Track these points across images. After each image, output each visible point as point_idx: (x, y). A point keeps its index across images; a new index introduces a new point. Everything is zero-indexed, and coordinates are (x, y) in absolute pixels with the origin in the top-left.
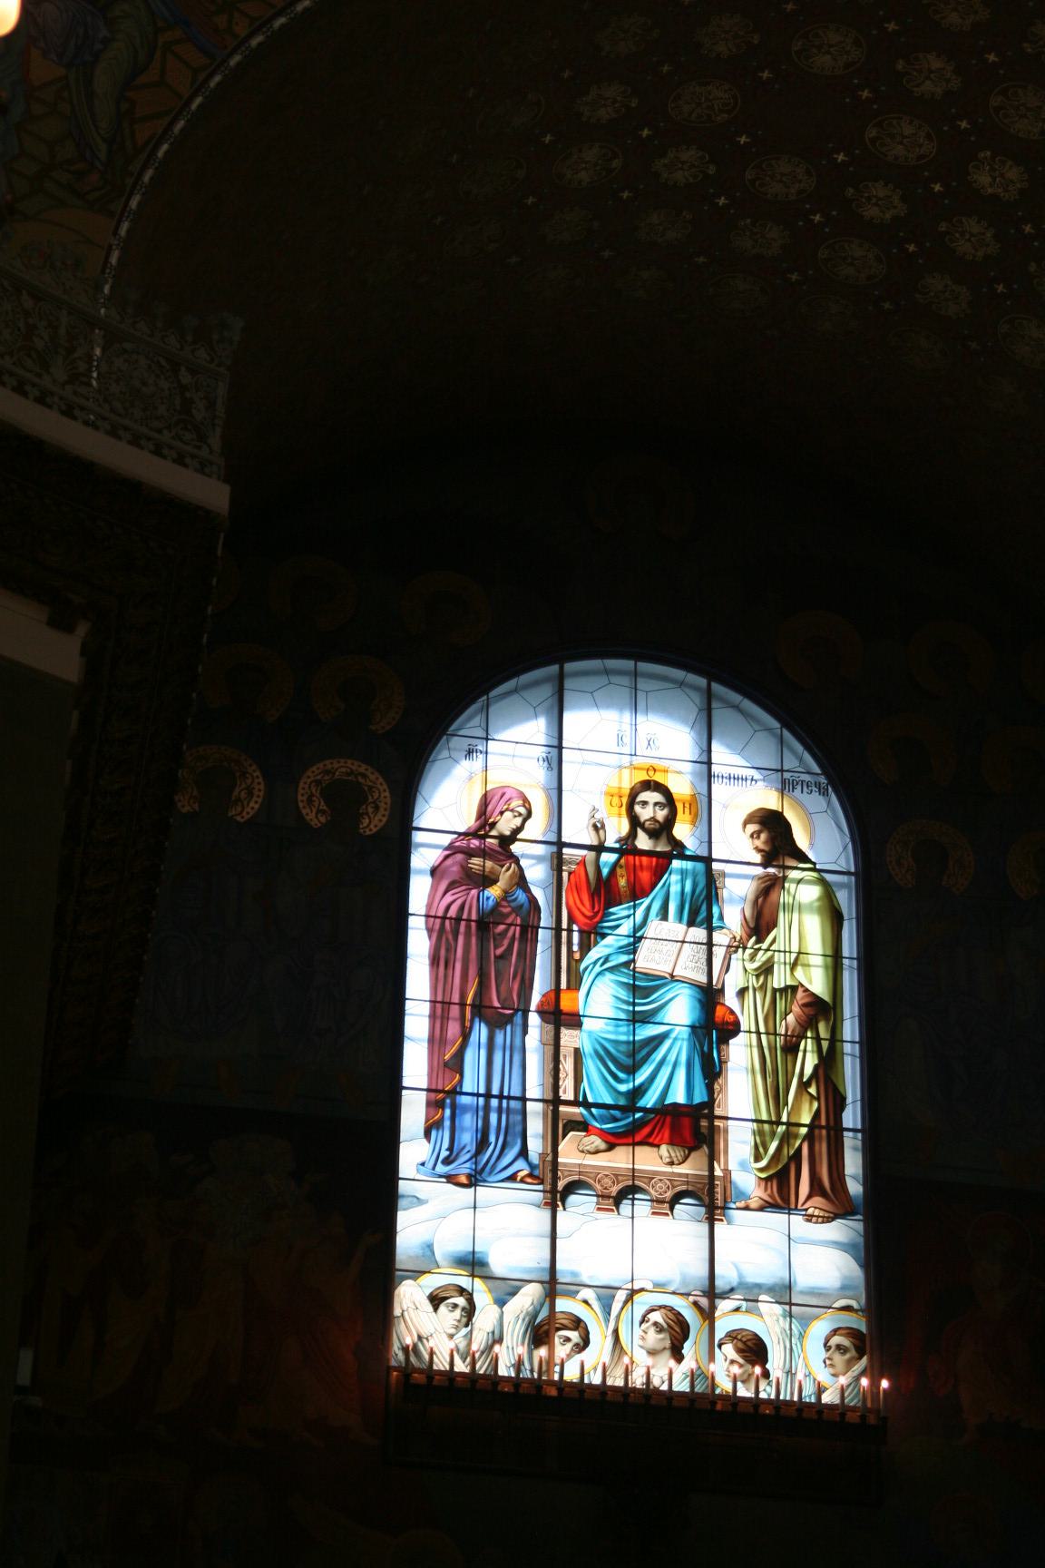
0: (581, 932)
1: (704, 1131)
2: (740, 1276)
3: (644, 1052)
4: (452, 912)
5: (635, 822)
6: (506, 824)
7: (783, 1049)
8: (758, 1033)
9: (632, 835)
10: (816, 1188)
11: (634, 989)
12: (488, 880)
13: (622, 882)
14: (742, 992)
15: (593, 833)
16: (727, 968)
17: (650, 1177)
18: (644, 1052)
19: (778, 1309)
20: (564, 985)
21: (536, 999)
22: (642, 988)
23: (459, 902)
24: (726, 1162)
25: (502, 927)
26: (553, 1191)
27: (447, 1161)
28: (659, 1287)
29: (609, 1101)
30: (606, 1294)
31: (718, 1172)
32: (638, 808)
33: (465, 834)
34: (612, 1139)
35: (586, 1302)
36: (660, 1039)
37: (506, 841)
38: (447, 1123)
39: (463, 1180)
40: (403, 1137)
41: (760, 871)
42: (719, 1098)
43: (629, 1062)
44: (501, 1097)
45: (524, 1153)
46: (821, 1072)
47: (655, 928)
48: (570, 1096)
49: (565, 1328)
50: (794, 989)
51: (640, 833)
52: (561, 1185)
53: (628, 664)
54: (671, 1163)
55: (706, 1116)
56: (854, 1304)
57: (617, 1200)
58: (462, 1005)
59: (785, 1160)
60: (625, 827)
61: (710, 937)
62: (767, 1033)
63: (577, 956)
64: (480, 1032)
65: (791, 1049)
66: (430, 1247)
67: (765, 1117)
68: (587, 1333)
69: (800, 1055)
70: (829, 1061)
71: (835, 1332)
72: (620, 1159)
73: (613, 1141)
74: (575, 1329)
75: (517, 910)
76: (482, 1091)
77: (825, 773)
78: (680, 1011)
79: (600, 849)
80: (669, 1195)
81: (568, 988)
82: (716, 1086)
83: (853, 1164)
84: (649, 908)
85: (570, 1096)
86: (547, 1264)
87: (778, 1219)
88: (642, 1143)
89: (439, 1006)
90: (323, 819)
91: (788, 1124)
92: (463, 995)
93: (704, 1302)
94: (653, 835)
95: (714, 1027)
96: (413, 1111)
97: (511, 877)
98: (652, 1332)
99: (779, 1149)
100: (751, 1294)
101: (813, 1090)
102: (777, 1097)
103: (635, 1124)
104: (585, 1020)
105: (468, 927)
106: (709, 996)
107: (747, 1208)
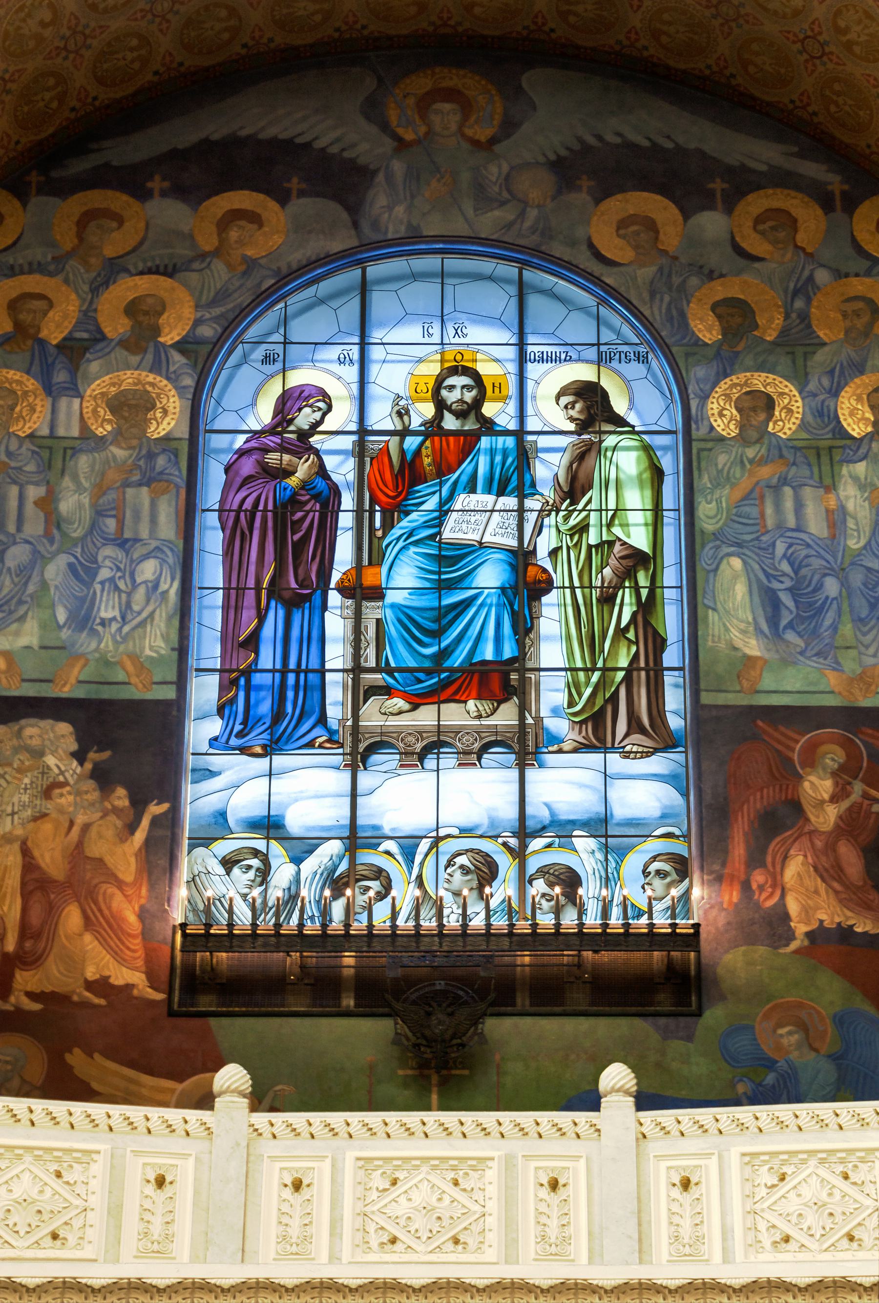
0: (383, 511)
2: (552, 813)
4: (248, 505)
5: (441, 406)
6: (304, 418)
7: (598, 600)
8: (572, 588)
10: (634, 725)
11: (440, 559)
13: (427, 461)
14: (554, 553)
15: (397, 420)
16: (539, 529)
17: (456, 731)
19: (592, 843)
21: (336, 577)
23: (255, 495)
24: (538, 710)
25: (299, 515)
26: (353, 753)
27: (241, 735)
28: (466, 832)
29: (412, 663)
31: (530, 721)
32: (444, 393)
34: (418, 701)
35: (388, 853)
36: (466, 604)
37: (304, 435)
39: (258, 750)
41: (573, 438)
43: (434, 626)
44: (297, 672)
45: (322, 720)
46: (640, 619)
47: (462, 501)
48: (372, 663)
50: (611, 544)
51: (447, 416)
54: (480, 717)
56: (677, 832)
57: (421, 759)
58: (258, 588)
61: (521, 504)
62: (582, 587)
63: (379, 534)
65: (608, 599)
66: (222, 814)
67: (579, 664)
69: (616, 609)
71: (654, 859)
72: (426, 717)
73: (416, 702)
75: (316, 497)
76: (278, 666)
78: (490, 576)
79: (404, 433)
80: (477, 746)
81: (370, 563)
82: (527, 641)
85: (372, 663)
86: (348, 822)
87: (595, 759)
89: (233, 593)
90: (109, 428)
91: (604, 670)
93: (513, 842)
94: (460, 415)
96: (204, 691)
98: (458, 876)
99: (593, 694)
101: (631, 635)
102: (592, 644)
104: (389, 593)
106: (521, 558)
107: (560, 751)
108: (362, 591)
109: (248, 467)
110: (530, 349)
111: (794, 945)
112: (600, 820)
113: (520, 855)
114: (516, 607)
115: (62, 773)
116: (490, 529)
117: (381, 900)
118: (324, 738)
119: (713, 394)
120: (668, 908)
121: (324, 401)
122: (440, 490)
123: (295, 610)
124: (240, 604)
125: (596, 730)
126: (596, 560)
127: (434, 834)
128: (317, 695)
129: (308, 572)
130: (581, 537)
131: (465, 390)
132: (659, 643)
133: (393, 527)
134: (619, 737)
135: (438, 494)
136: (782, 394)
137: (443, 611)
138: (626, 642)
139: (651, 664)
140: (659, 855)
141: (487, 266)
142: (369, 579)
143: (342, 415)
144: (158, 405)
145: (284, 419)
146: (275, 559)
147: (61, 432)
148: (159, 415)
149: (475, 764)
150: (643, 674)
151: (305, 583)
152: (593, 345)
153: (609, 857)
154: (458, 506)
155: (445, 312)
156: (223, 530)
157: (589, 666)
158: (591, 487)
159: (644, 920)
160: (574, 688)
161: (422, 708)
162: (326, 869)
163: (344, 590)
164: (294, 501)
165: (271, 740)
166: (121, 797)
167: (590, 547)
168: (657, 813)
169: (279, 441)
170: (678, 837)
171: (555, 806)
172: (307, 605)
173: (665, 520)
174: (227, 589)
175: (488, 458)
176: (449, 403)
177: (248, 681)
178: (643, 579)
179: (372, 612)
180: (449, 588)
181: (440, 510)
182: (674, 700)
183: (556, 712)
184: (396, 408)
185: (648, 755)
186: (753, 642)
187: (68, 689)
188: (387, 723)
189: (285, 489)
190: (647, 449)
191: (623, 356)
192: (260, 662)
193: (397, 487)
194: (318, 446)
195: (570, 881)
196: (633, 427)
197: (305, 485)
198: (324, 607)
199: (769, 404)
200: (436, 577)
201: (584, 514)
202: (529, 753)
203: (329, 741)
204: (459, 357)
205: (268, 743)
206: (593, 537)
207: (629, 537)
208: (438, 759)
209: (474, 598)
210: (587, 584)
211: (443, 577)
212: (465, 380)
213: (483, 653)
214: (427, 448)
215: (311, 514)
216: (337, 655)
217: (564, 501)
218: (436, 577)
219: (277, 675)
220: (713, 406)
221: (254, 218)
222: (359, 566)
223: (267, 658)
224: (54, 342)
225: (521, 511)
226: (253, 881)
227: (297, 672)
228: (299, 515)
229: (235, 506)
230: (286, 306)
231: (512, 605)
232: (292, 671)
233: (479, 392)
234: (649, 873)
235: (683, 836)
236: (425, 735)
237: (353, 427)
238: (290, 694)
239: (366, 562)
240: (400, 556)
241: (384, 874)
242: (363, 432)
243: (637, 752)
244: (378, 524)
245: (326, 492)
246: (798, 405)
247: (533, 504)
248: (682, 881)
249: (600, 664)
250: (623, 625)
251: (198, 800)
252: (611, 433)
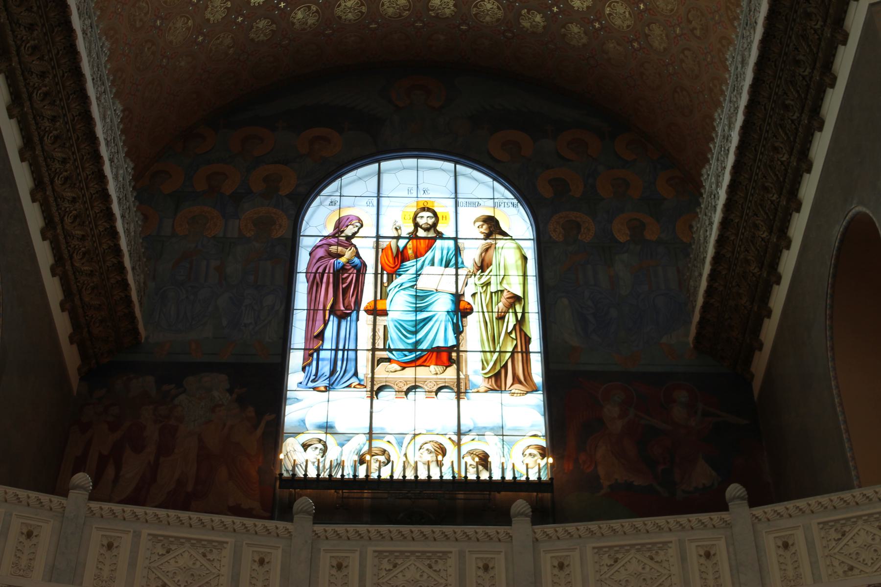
2: (475, 424)
3: (421, 325)
4: (320, 270)
5: (417, 226)
8: (483, 312)
9: (416, 230)
10: (516, 380)
11: (416, 297)
12: (340, 256)
13: (410, 252)
14: (474, 295)
18: (421, 325)
20: (379, 297)
21: (364, 305)
22: (421, 299)
24: (466, 371)
25: (346, 275)
26: (372, 391)
27: (313, 381)
28: (429, 432)
29: (402, 347)
31: (462, 376)
32: (418, 220)
33: (328, 236)
38: (314, 363)
39: (323, 389)
40: (290, 371)
42: (462, 343)
43: (414, 329)
44: (344, 350)
45: (356, 374)
46: (517, 328)
47: (427, 269)
48: (382, 347)
49: (377, 454)
50: (502, 291)
53: (412, 162)
55: (455, 351)
56: (540, 434)
57: (407, 393)
58: (324, 310)
59: (498, 368)
60: (411, 228)
63: (386, 285)
64: (333, 322)
65: (501, 318)
66: (303, 421)
67: (487, 349)
68: (390, 456)
72: (409, 373)
73: (404, 366)
75: (355, 267)
76: (334, 347)
77: (516, 198)
78: (442, 305)
79: (398, 238)
80: (435, 389)
82: (461, 337)
84: (424, 261)
85: (382, 347)
86: (368, 425)
87: (496, 396)
89: (312, 312)
91: (500, 352)
92: (325, 306)
93: (455, 438)
94: (426, 230)
95: (460, 311)
96: (296, 359)
101: (513, 335)
106: (457, 297)
107: (478, 392)
108: (376, 312)
109: (321, 252)
125: (497, 380)
126: (495, 299)
128: (353, 363)
129: (349, 303)
132: (527, 340)
134: (508, 386)
142: (380, 306)
143: (369, 229)
145: (339, 231)
150: (520, 355)
158: (491, 264)
160: (485, 362)
163: (368, 311)
164: (343, 269)
167: (492, 293)
174: (309, 310)
178: (519, 309)
179: (381, 321)
180: (421, 311)
183: (475, 372)
190: (520, 248)
197: (349, 261)
203: (359, 384)
209: (432, 317)
212: (430, 214)
216: (365, 342)
219: (333, 352)
222: (375, 300)
223: (327, 345)
225: (457, 275)
227: (344, 350)
228: (346, 275)
229: (314, 271)
237: (375, 235)
238: (339, 363)
239: (379, 297)
244: (385, 280)
245: (359, 264)
249: (498, 349)
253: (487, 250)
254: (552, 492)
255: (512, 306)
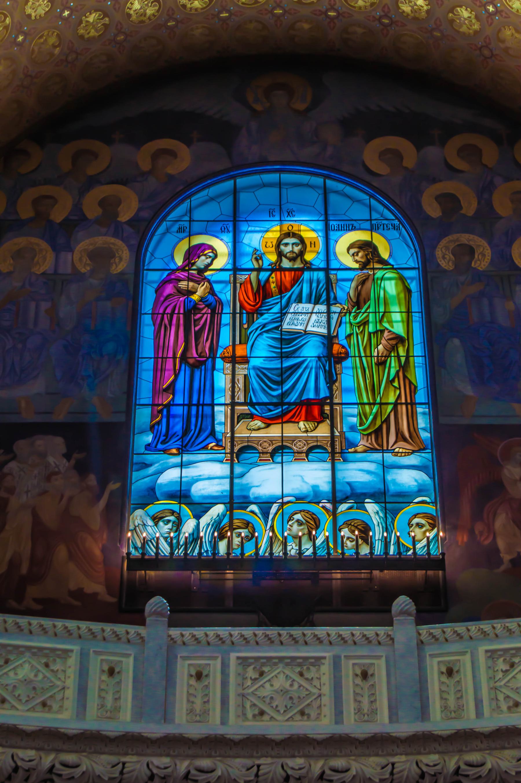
0: (248, 313)
1: (328, 412)
3: (288, 373)
4: (169, 311)
5: (280, 255)
7: (376, 364)
8: (360, 357)
11: (281, 340)
13: (273, 286)
14: (349, 337)
15: (255, 263)
16: (340, 323)
17: (293, 440)
18: (288, 373)
20: (238, 342)
23: (173, 305)
24: (342, 428)
25: (198, 316)
26: (232, 453)
27: (164, 442)
28: (300, 499)
29: (265, 400)
30: (265, 506)
31: (337, 434)
32: (282, 247)
35: (252, 512)
36: (297, 366)
39: (174, 451)
41: (358, 272)
43: (279, 379)
44: (198, 405)
45: (213, 433)
46: (401, 374)
48: (242, 400)
49: (240, 528)
50: (382, 332)
52: (236, 449)
54: (307, 431)
55: (327, 404)
57: (272, 456)
59: (378, 423)
62: (366, 356)
65: (381, 363)
67: (365, 400)
70: (404, 367)
72: (275, 431)
73: (269, 422)
74: (247, 528)
78: (311, 351)
79: (260, 270)
80: (305, 449)
81: (240, 343)
82: (334, 387)
83: (422, 422)
85: (242, 400)
87: (378, 456)
88: (288, 422)
89: (160, 360)
90: (88, 268)
91: (381, 404)
92: (175, 354)
93: (329, 506)
94: (293, 260)
95: (333, 357)
96: (143, 416)
97: (205, 289)
98: (295, 527)
99: (375, 418)
100: (358, 497)
103: (284, 411)
105: (178, 319)
107: (356, 452)
110: (331, 223)
111: (503, 568)
112: (381, 493)
113: (334, 514)
114: (327, 368)
115: (57, 466)
116: (311, 324)
117: (249, 541)
118: (214, 444)
119: (439, 246)
120: (425, 546)
121: (212, 252)
122: (281, 302)
123: (196, 370)
124: (164, 367)
126: (374, 341)
127: (280, 501)
128: (209, 420)
130: (364, 328)
131: (294, 246)
132: (413, 389)
133: (253, 322)
134: (391, 444)
135: (279, 304)
136: (479, 246)
137: (284, 370)
138: (393, 388)
139: (409, 401)
140: (418, 514)
141: (305, 178)
144: (117, 255)
146: (185, 341)
147: (60, 271)
148: (117, 260)
149: (304, 459)
150: (404, 407)
151: (202, 354)
152: (368, 220)
153: (388, 515)
154: (292, 310)
155: (282, 203)
156: (154, 325)
157: (371, 401)
158: (369, 299)
159: (410, 552)
161: (272, 426)
162: (215, 521)
165: (182, 445)
166: (92, 480)
167: (370, 334)
168: (416, 489)
169: (187, 275)
170: (428, 503)
171: (353, 484)
172: (203, 367)
173: (414, 318)
174: (156, 358)
175: (309, 285)
176: (285, 253)
177: (168, 411)
178: (402, 352)
179: (241, 370)
180: (287, 357)
181: (281, 313)
182: (422, 422)
184: (255, 256)
185: (409, 454)
186: (469, 388)
187: (60, 416)
188: (251, 435)
189: (190, 302)
190: (402, 279)
191: (385, 226)
192: (175, 400)
193: (256, 300)
194: (209, 278)
195: (364, 531)
196: (393, 266)
198: (214, 368)
199: (471, 251)
200: (279, 350)
201: (366, 314)
202: (337, 453)
204: (290, 228)
205: (180, 447)
206: (371, 328)
207: (392, 327)
208: (282, 456)
209: (302, 362)
210: (368, 354)
211: (283, 350)
213: (308, 394)
214: (273, 278)
215: (206, 315)
217: (354, 307)
218: (279, 350)
219: (186, 407)
220: (439, 253)
221: (172, 154)
224: (58, 221)
225: (329, 313)
226: (171, 529)
227: (198, 405)
229: (161, 311)
230: (191, 201)
231: (324, 367)
232: (194, 405)
233: (303, 246)
234: (412, 525)
235: (432, 503)
236: (274, 442)
238: (193, 420)
239: (238, 342)
240: (258, 339)
241: (250, 525)
242: (236, 269)
243: (402, 453)
244: (245, 322)
246: (488, 252)
247: (335, 309)
248: (432, 530)
250: (391, 378)
251: (139, 481)
252: (380, 269)
253: (363, 283)
254: (444, 569)
255: (394, 348)
